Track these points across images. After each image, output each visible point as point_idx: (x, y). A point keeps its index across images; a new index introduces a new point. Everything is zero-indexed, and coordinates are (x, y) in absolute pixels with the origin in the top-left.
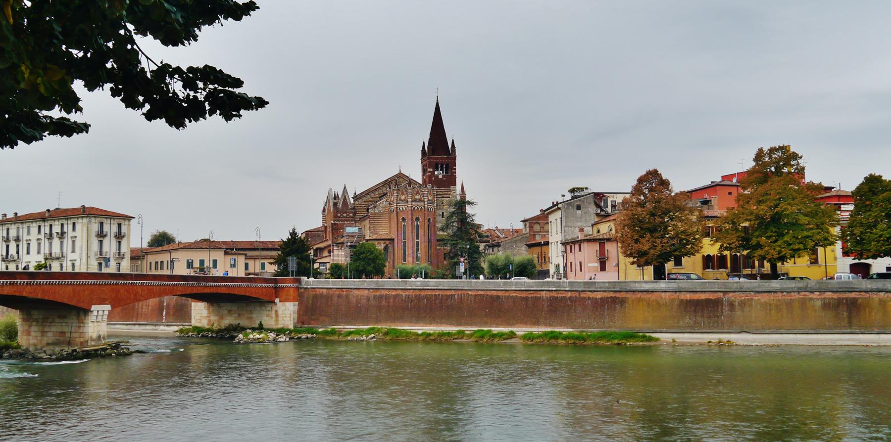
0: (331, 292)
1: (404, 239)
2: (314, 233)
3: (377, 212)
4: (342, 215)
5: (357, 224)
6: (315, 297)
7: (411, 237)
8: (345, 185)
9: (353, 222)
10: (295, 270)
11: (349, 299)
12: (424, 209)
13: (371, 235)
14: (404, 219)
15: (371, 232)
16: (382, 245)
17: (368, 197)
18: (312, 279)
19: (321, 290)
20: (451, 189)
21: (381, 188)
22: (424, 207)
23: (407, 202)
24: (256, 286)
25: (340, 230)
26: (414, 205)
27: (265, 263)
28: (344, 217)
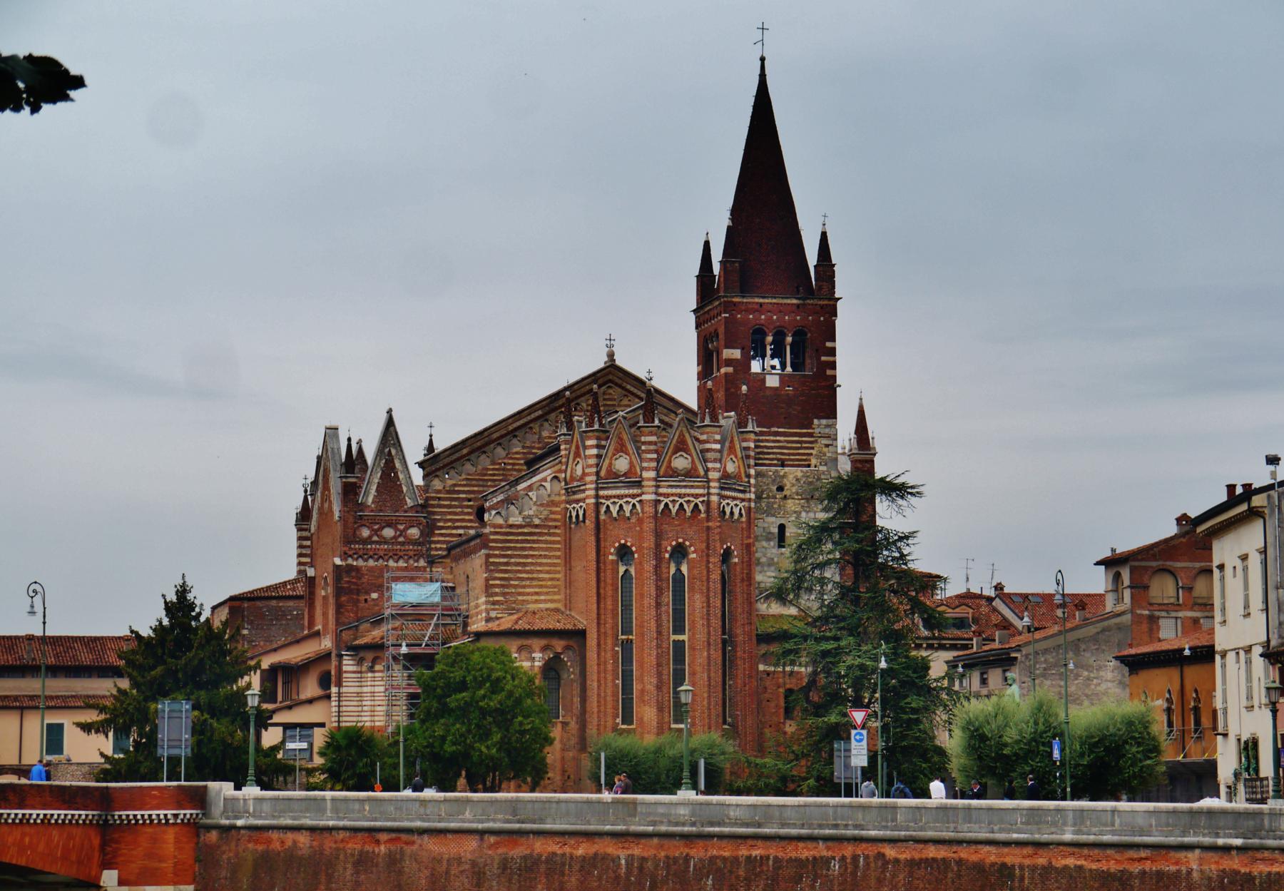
0: (329, 844)
1: (627, 630)
2: (259, 604)
3: (516, 519)
4: (376, 532)
5: (438, 570)
6: (266, 862)
7: (653, 624)
8: (389, 412)
9: (422, 563)
10: (184, 752)
11: (400, 872)
12: (708, 511)
13: (493, 614)
14: (624, 553)
15: (494, 603)
16: (538, 655)
17: (484, 461)
18: (252, 791)
19: (290, 836)
20: (817, 431)
21: (536, 427)
22: (708, 503)
23: (638, 484)
24: (25, 821)
25: (368, 593)
26: (667, 495)
27: (61, 726)
28: (384, 541)
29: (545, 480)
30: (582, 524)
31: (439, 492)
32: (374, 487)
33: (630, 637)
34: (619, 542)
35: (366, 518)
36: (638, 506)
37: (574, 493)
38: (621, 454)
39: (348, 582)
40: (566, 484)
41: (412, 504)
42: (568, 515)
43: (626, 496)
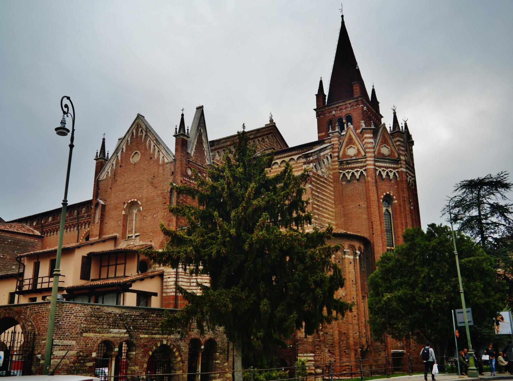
8: (200, 109)
29: (327, 154)
30: (356, 181)
31: (218, 161)
32: (194, 147)
33: (393, 248)
34: (386, 193)
35: (191, 163)
36: (397, 174)
37: (348, 164)
38: (385, 145)
39: (182, 200)
40: (339, 159)
41: (208, 164)
42: (341, 176)
43: (390, 168)
